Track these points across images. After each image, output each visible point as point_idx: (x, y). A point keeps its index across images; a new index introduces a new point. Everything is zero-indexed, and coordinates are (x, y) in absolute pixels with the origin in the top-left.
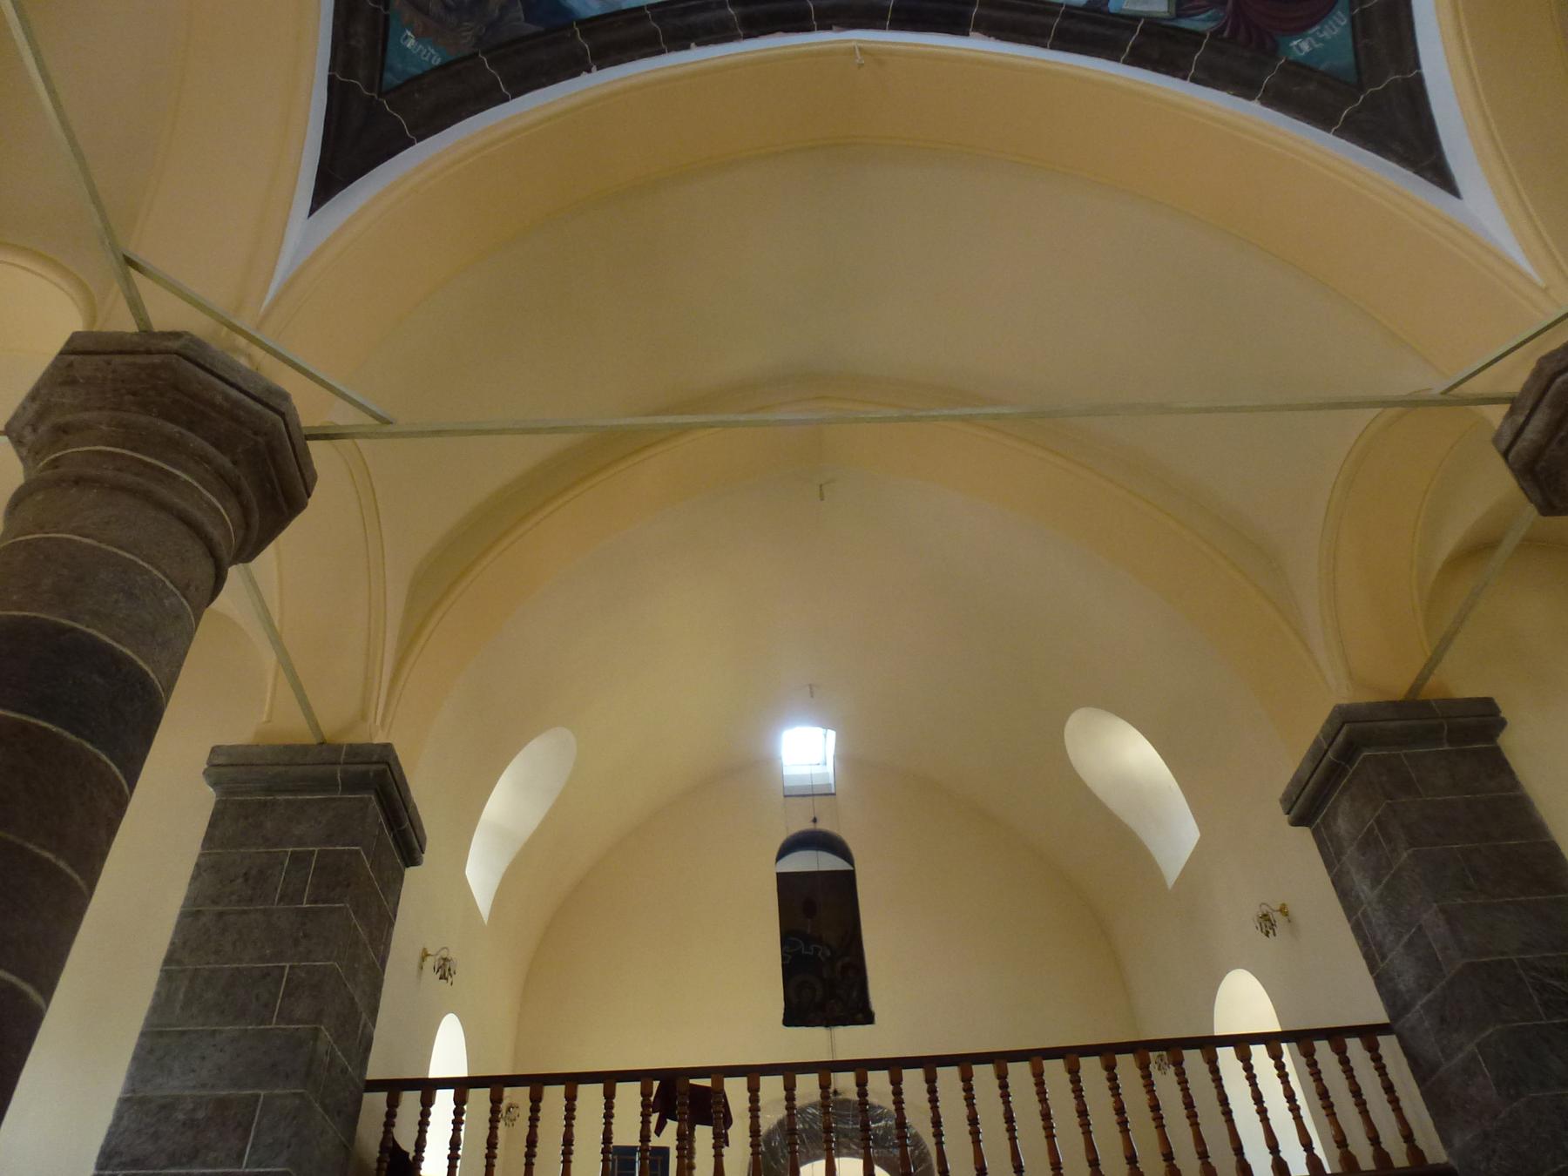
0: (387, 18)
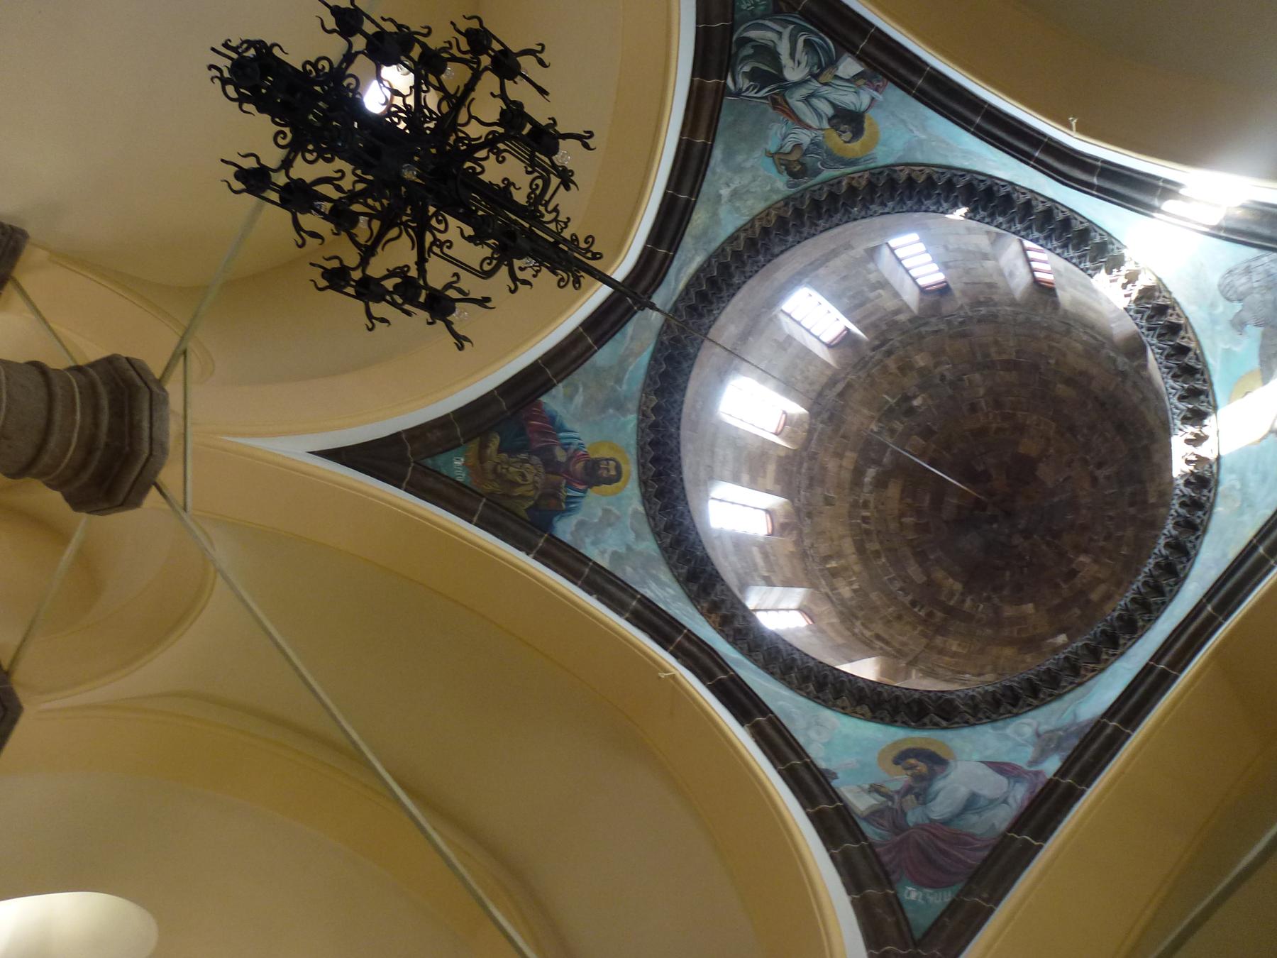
0: (459, 445)
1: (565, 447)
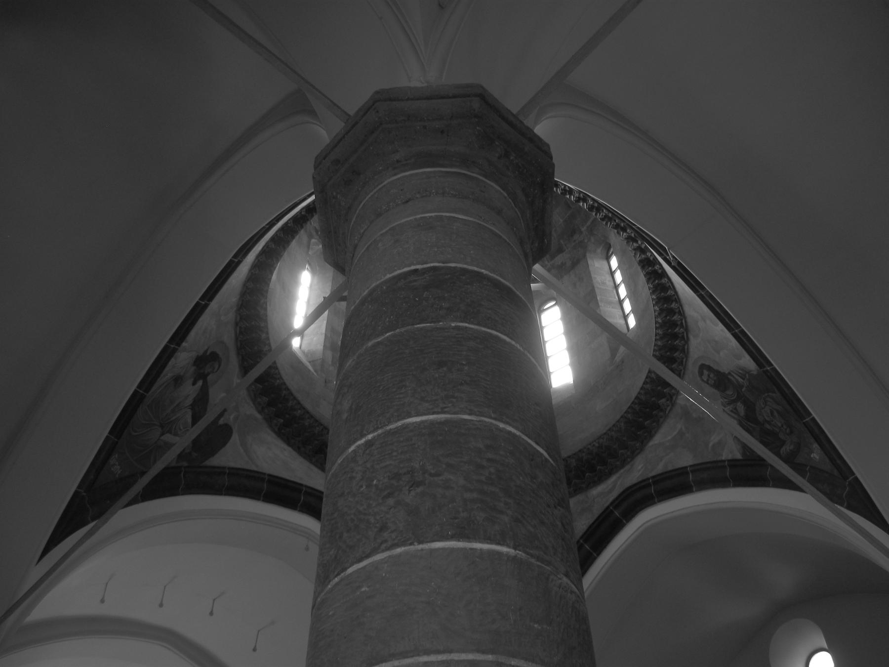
1: (735, 411)
